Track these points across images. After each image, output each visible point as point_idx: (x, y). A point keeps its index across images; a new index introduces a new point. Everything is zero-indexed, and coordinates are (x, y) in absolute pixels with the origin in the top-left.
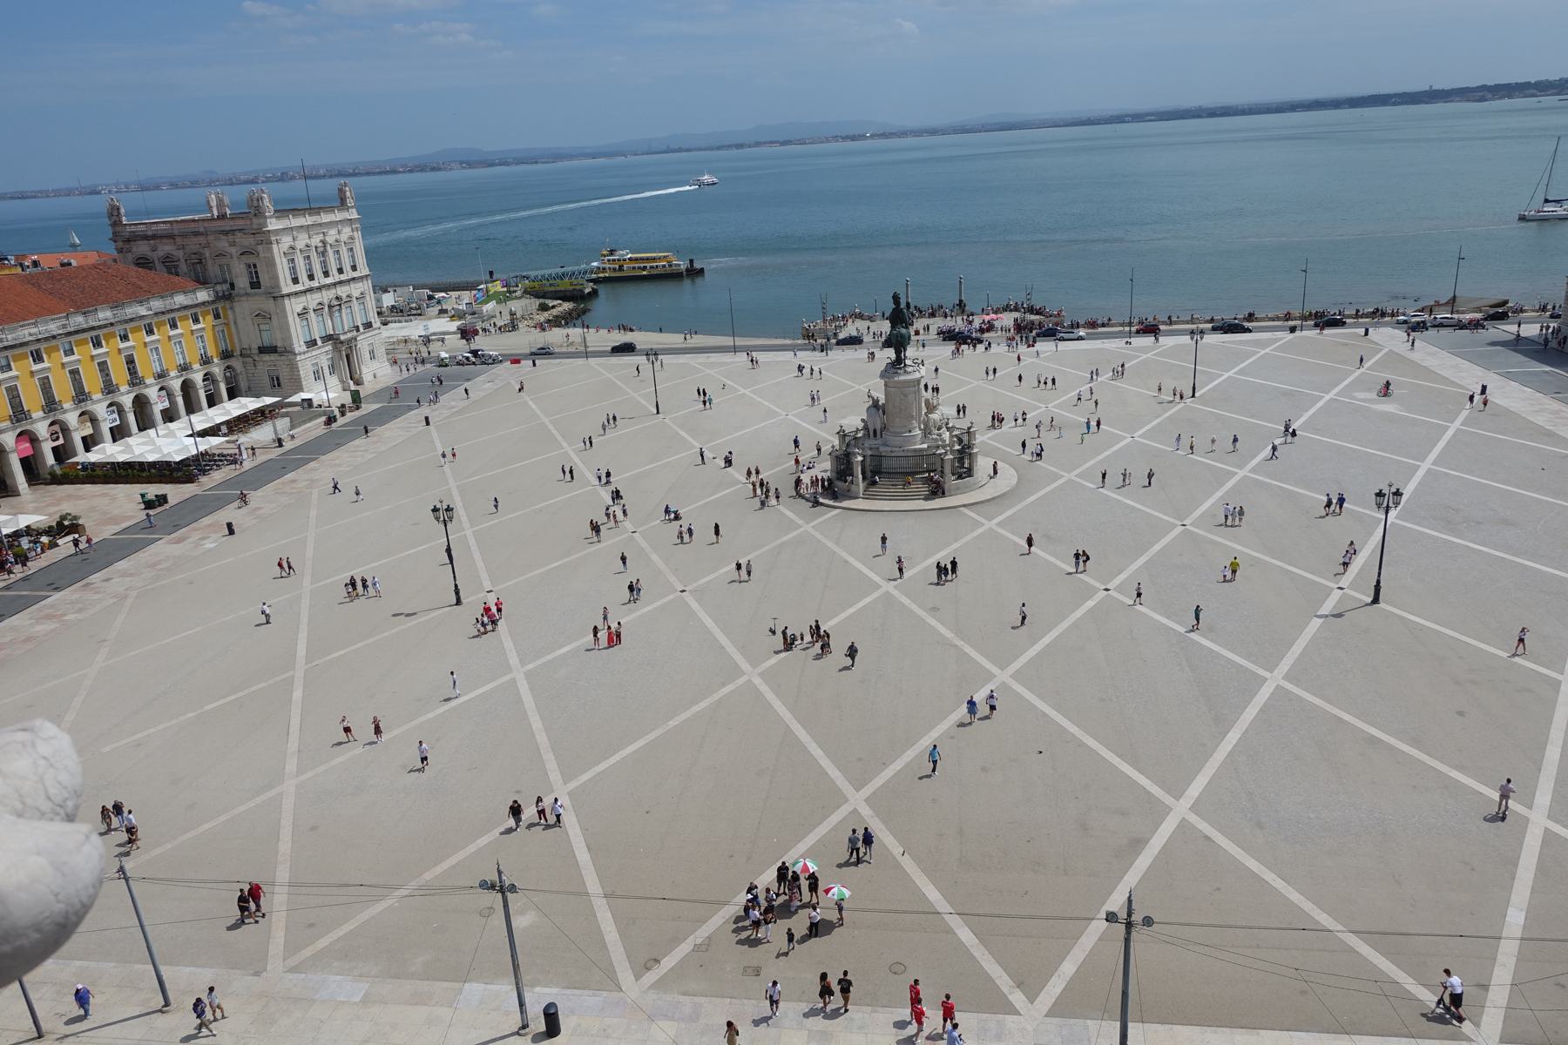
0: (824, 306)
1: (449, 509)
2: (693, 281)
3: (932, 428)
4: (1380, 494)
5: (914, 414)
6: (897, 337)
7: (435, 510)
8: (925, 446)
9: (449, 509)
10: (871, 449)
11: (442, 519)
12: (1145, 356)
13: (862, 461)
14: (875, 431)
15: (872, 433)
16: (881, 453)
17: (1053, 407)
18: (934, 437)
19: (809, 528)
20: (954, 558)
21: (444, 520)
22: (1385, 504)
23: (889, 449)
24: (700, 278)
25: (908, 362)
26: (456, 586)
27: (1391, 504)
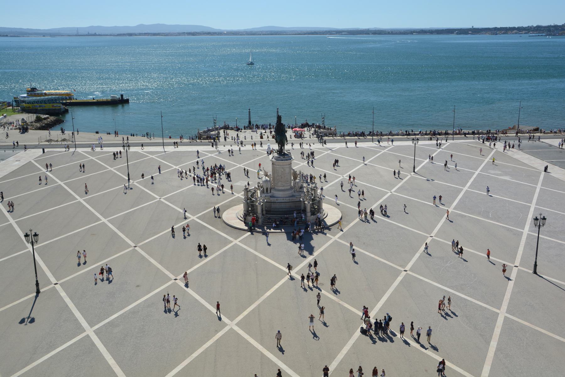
0: (215, 122)
1: (36, 235)
2: (123, 106)
4: (536, 219)
7: (26, 236)
9: (36, 235)
11: (31, 241)
12: (383, 151)
14: (267, 189)
17: (346, 177)
19: (237, 242)
21: (32, 242)
22: (538, 225)
23: (276, 199)
24: (127, 105)
26: (37, 281)
27: (541, 224)
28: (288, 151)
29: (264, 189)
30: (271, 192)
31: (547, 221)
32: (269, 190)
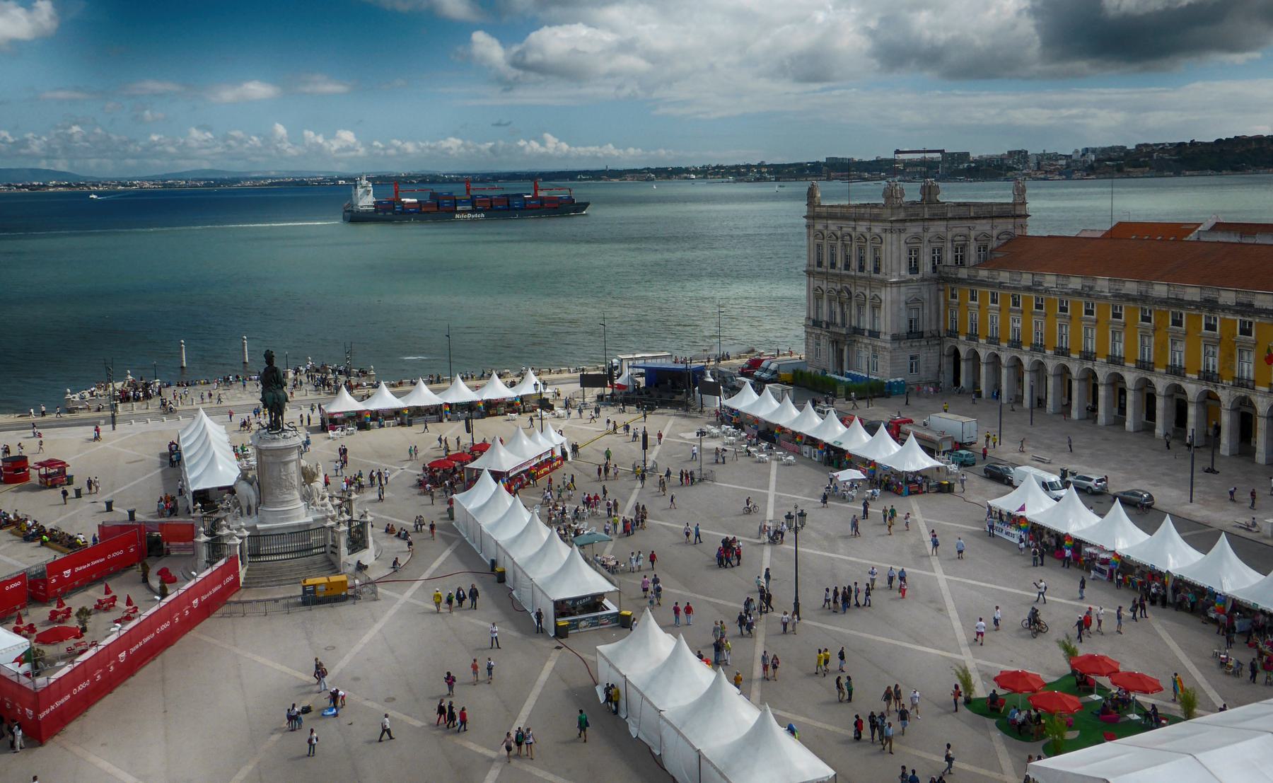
3: (316, 499)
5: (296, 484)
6: (274, 399)
8: (310, 519)
10: (247, 529)
13: (240, 545)
15: (245, 511)
16: (259, 531)
18: (319, 508)
20: (688, 603)
25: (286, 427)
27: (799, 526)
28: (291, 425)
29: (241, 509)
30: (257, 513)
31: (808, 520)
32: (253, 510)
